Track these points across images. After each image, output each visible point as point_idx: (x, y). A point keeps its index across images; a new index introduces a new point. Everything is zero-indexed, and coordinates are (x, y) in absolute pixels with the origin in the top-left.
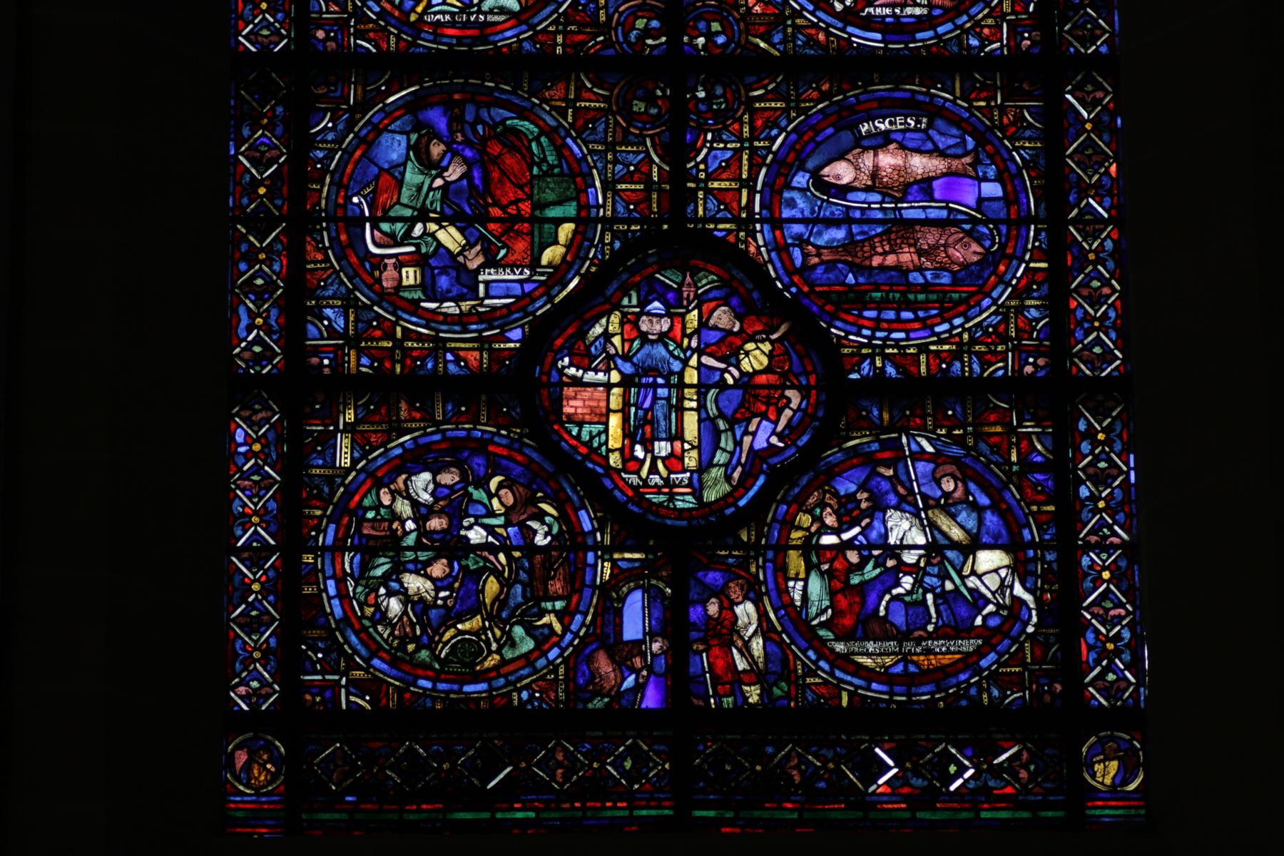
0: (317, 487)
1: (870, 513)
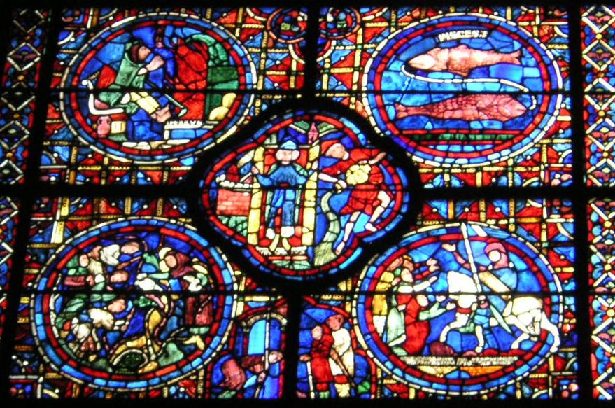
0: (36, 255)
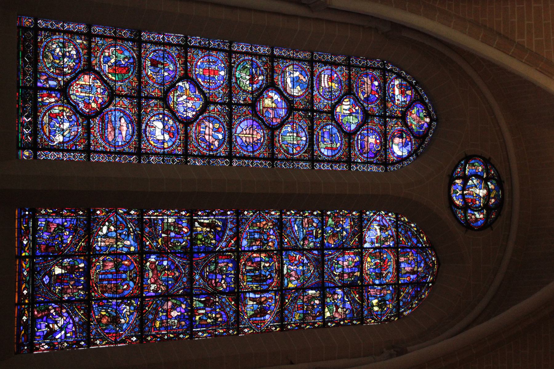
1: (69, 120)
